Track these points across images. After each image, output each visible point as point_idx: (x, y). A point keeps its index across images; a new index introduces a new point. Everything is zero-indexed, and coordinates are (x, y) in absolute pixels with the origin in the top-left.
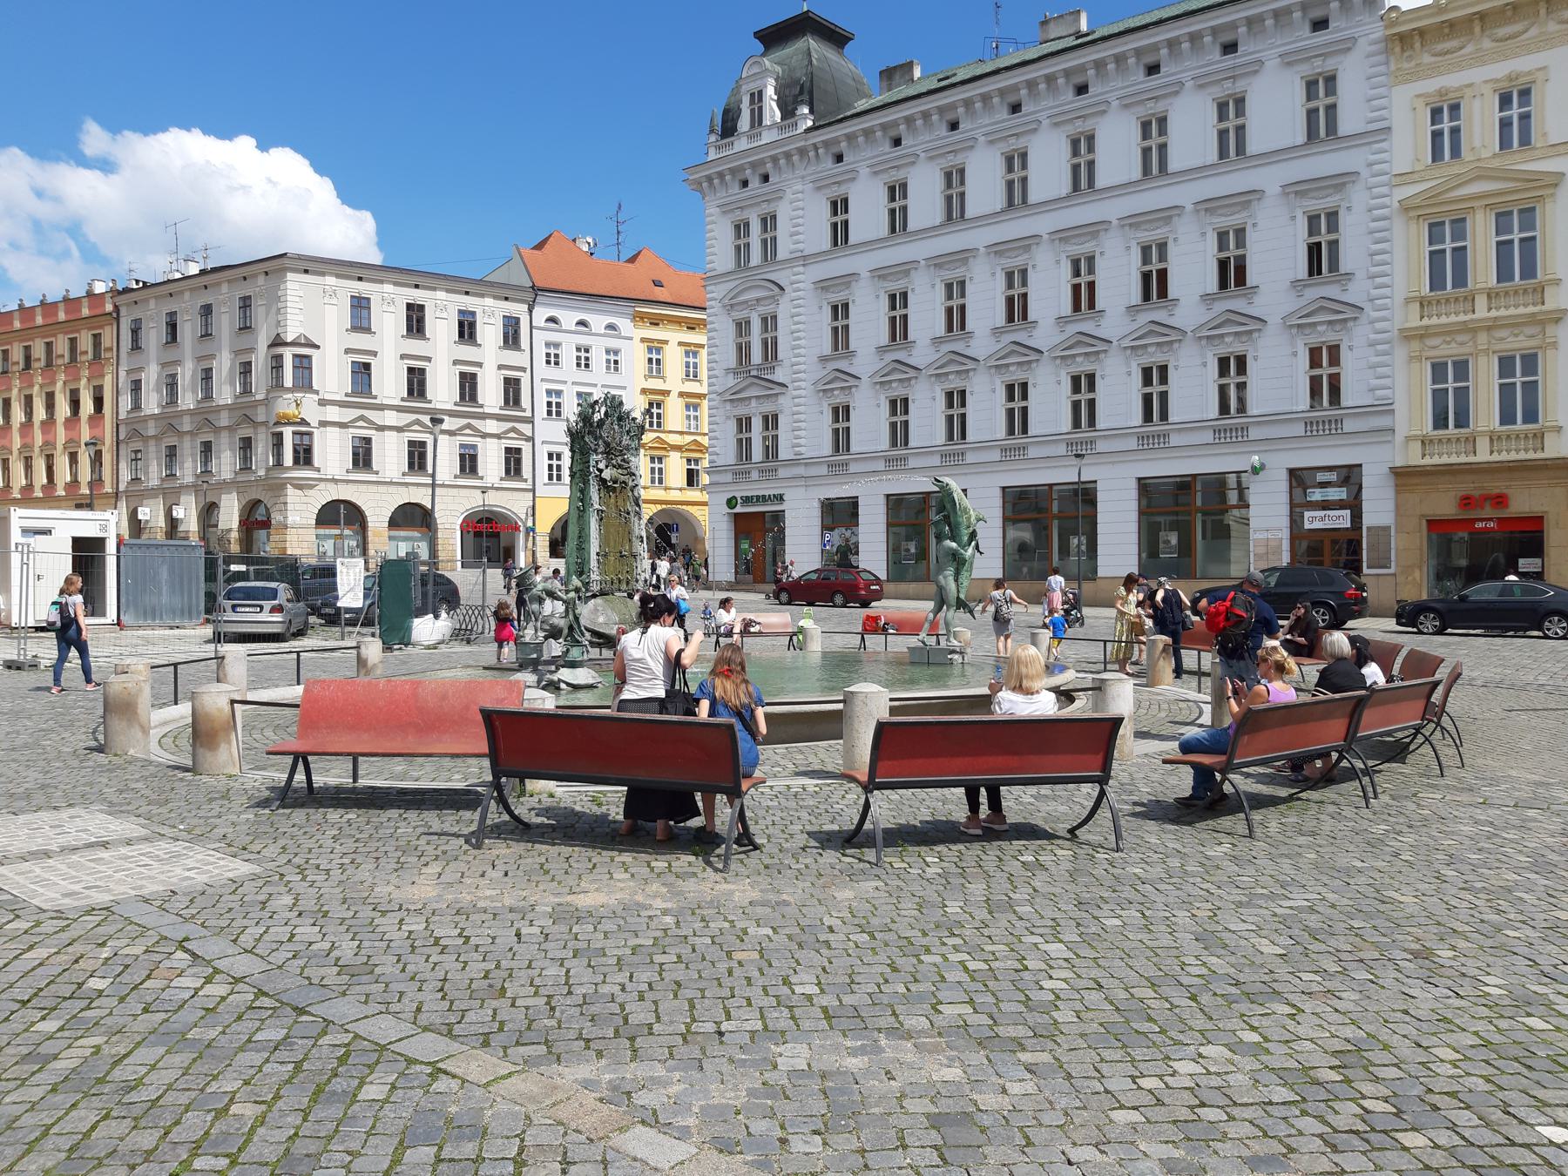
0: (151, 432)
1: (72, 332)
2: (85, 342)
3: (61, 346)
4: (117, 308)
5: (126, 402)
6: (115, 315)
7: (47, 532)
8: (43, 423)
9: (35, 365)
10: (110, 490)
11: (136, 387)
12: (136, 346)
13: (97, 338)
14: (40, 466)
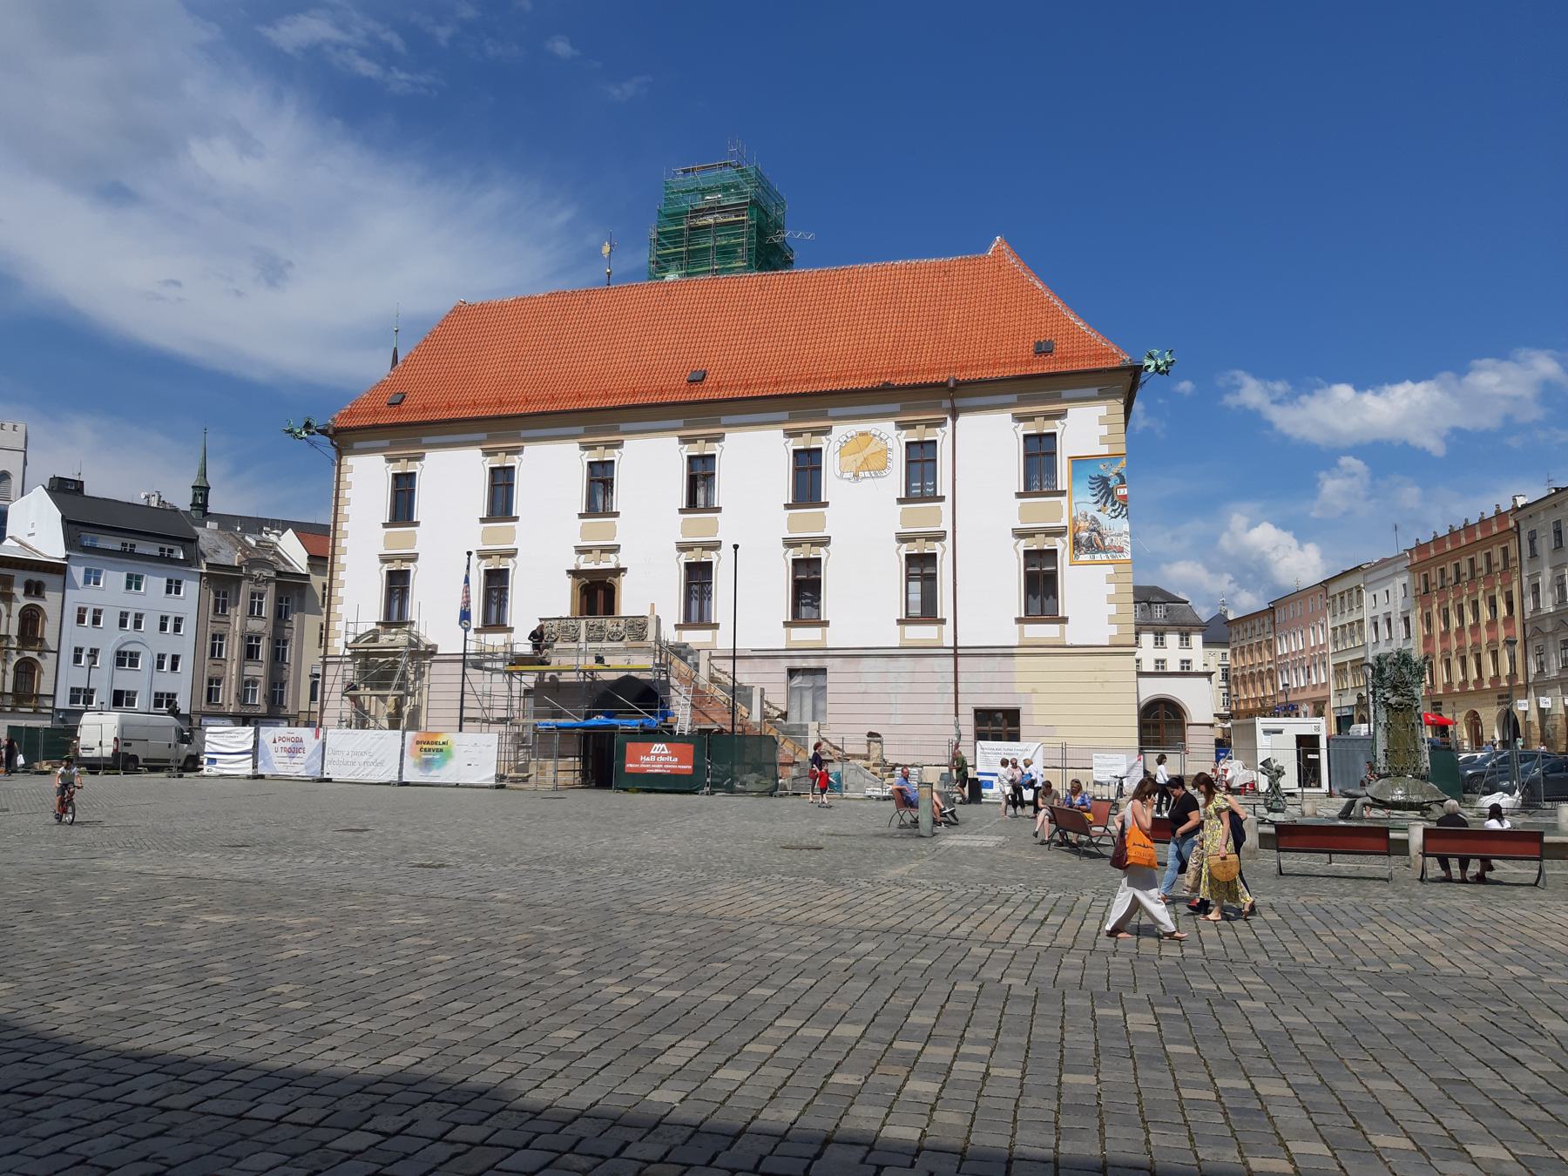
0: (1549, 629)
1: (1470, 554)
2: (1497, 556)
3: (1481, 562)
4: (1517, 524)
5: (1529, 604)
6: (1515, 530)
7: (1280, 732)
8: (1472, 627)
9: (1463, 579)
10: (1522, 682)
11: (1536, 589)
12: (1534, 555)
13: (1505, 550)
14: (1472, 662)
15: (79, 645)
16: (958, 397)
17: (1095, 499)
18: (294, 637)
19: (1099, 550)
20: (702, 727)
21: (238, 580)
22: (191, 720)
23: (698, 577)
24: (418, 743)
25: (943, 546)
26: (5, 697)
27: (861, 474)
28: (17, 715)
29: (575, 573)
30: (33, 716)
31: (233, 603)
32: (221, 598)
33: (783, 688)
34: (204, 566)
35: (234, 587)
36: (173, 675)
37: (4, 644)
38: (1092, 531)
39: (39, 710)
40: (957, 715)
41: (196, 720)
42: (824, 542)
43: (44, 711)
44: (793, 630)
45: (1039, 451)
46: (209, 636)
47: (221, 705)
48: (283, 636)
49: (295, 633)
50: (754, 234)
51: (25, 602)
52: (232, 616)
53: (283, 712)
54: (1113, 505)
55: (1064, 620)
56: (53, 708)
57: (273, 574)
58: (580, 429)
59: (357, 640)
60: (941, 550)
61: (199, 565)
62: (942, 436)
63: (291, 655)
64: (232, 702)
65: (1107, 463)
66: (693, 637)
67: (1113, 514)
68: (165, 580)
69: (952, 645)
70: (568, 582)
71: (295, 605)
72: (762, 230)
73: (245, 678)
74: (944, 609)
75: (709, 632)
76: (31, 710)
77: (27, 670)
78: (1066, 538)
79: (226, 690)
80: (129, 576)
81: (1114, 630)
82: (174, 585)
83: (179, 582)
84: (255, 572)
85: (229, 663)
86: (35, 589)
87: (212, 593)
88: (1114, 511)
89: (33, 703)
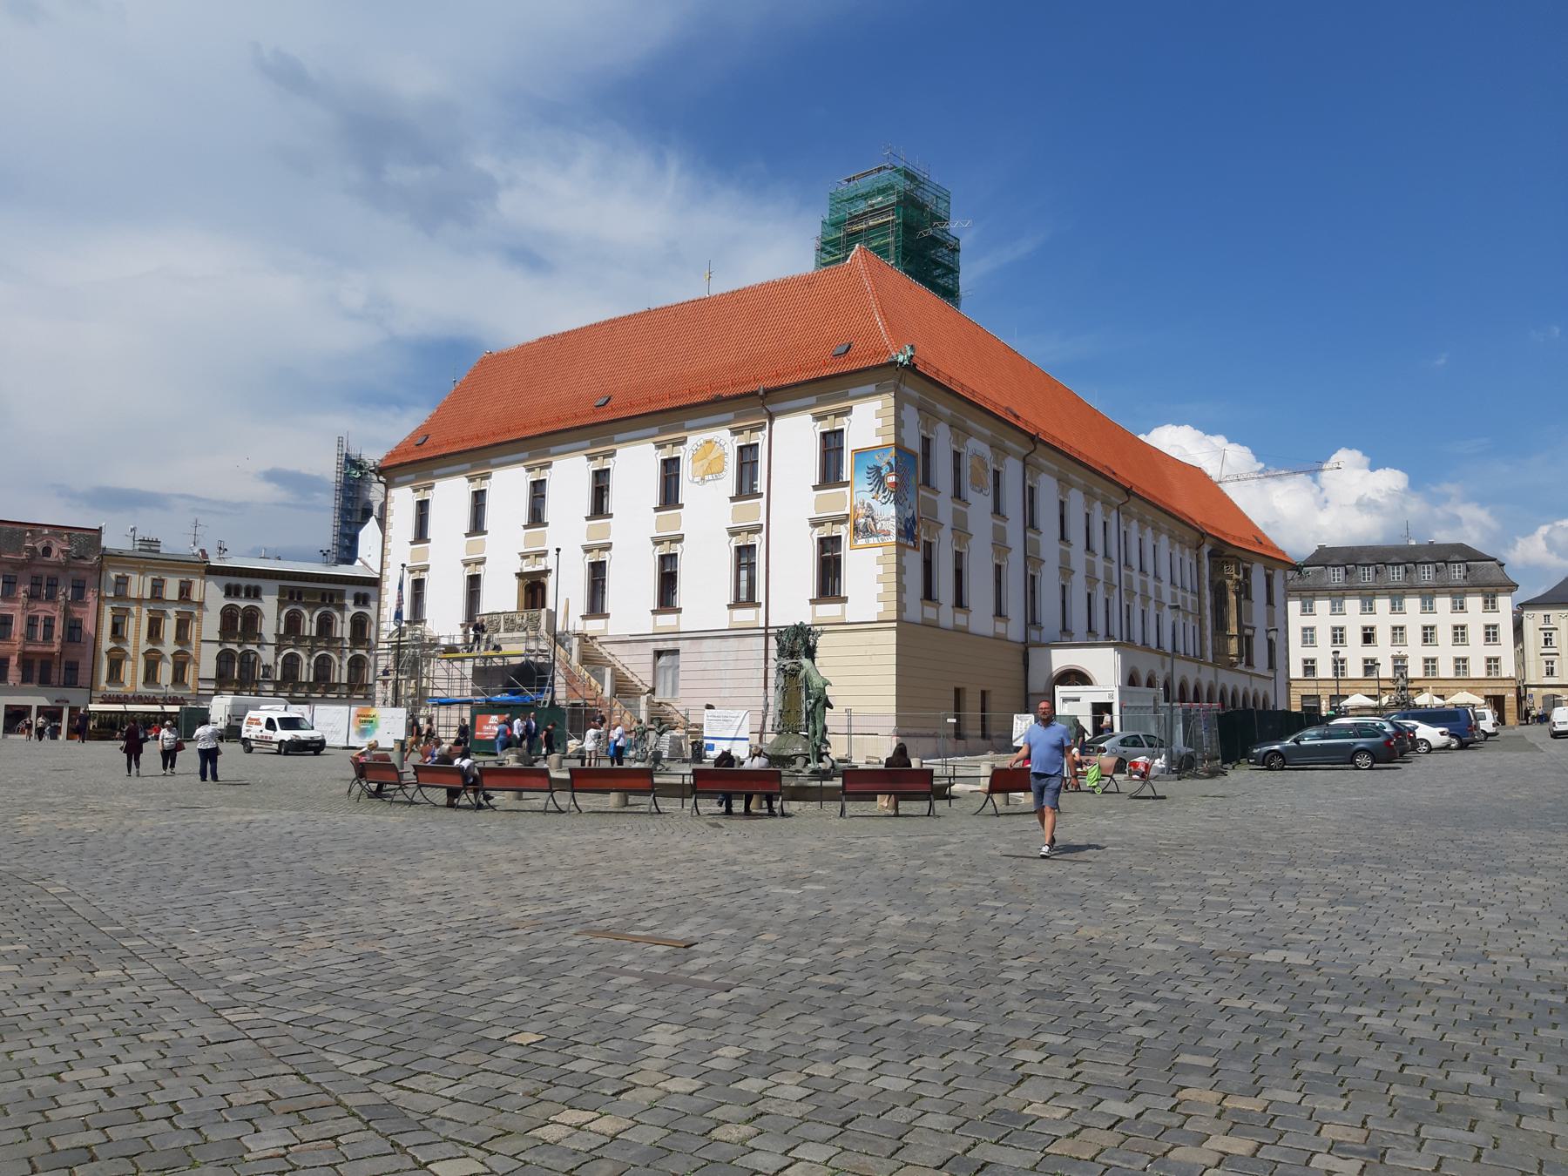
16: (772, 403)
17: (872, 486)
19: (872, 534)
20: (575, 702)
23: (597, 572)
24: (359, 716)
25: (760, 538)
27: (707, 477)
29: (520, 575)
33: (650, 667)
37: (339, 644)
38: (868, 517)
40: (766, 687)
42: (679, 539)
44: (659, 617)
45: (831, 444)
50: (901, 232)
51: (354, 610)
54: (884, 492)
55: (845, 600)
58: (525, 455)
59: (390, 636)
60: (758, 540)
62: (760, 438)
65: (880, 454)
66: (593, 626)
67: (883, 501)
69: (764, 626)
70: (515, 582)
72: (909, 228)
74: (760, 596)
75: (603, 621)
76: (362, 697)
77: (357, 664)
78: (848, 525)
81: (880, 607)
86: (362, 600)
88: (884, 497)
89: (363, 691)
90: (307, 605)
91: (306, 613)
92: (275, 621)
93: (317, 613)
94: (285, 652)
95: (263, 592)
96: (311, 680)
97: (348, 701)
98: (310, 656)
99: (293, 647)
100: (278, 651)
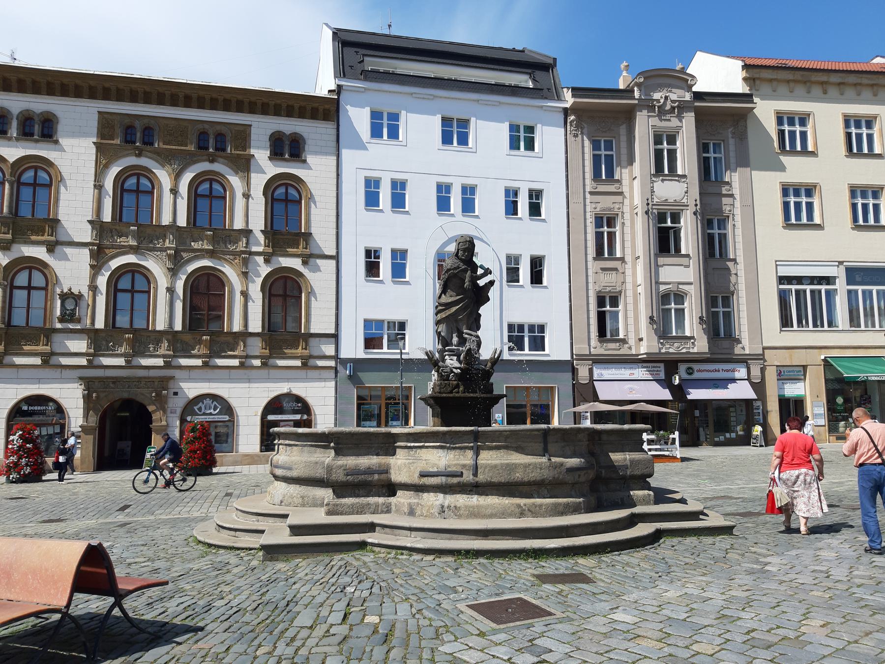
15: (373, 245)
18: (737, 211)
21: (628, 116)
22: (574, 371)
26: (251, 341)
28: (273, 372)
30: (302, 373)
31: (624, 157)
32: (603, 153)
34: (568, 95)
35: (623, 130)
36: (537, 291)
37: (241, 246)
39: (312, 362)
41: (583, 372)
43: (320, 363)
46: (590, 220)
47: (624, 341)
48: (720, 210)
49: (737, 204)
51: (272, 169)
52: (626, 182)
53: (738, 350)
56: (336, 357)
57: (688, 97)
61: (559, 98)
63: (737, 246)
64: (643, 334)
68: (506, 126)
71: (732, 154)
73: (662, 288)
76: (298, 363)
79: (631, 314)
80: (446, 121)
82: (522, 134)
83: (530, 129)
84: (657, 96)
85: (629, 266)
87: (587, 143)
89: (299, 351)
90: (165, 158)
91: (164, 176)
92: (90, 192)
93: (187, 177)
94: (115, 264)
95: (61, 128)
96: (178, 326)
97: (264, 372)
98: (173, 272)
99: (135, 250)
100: (99, 256)
